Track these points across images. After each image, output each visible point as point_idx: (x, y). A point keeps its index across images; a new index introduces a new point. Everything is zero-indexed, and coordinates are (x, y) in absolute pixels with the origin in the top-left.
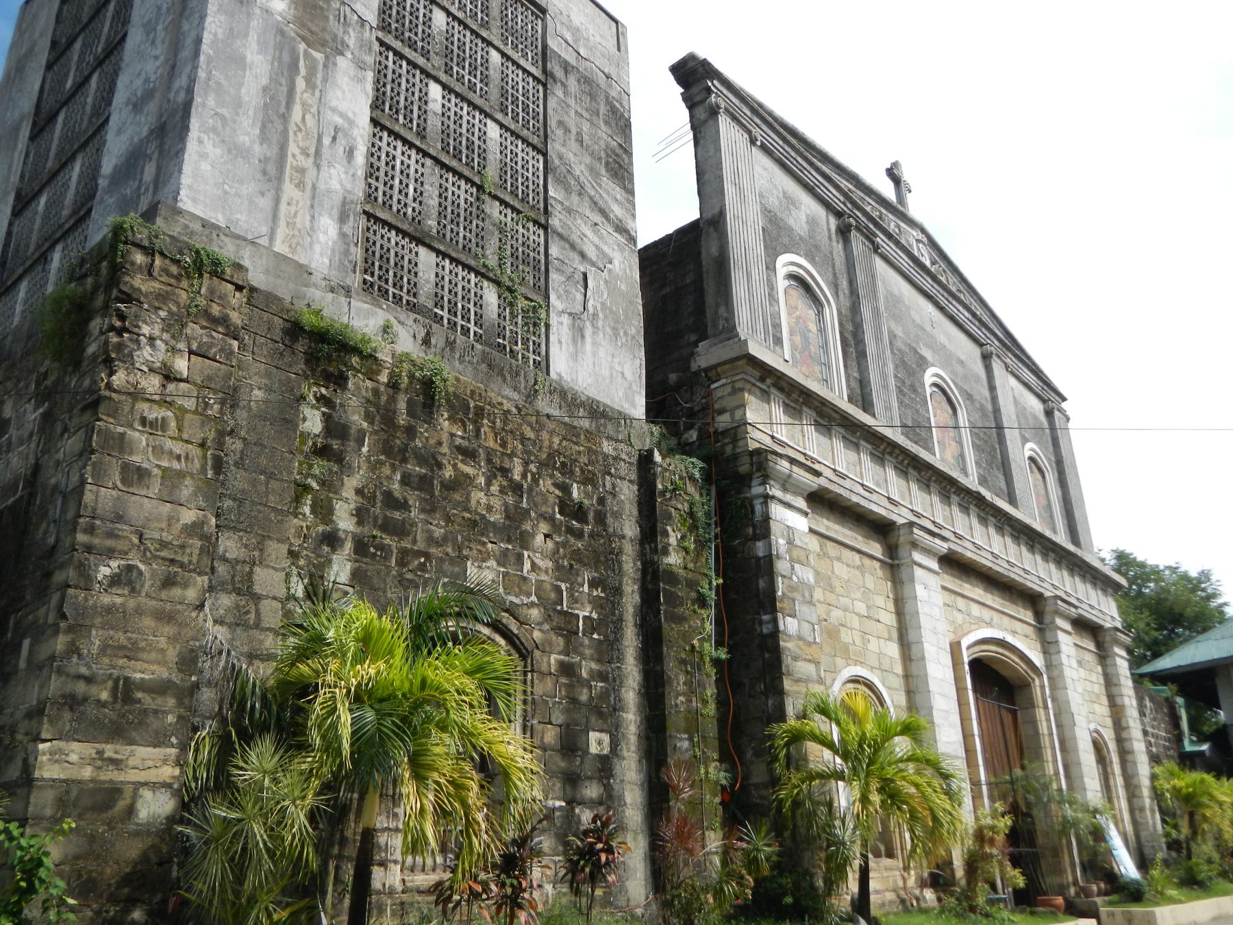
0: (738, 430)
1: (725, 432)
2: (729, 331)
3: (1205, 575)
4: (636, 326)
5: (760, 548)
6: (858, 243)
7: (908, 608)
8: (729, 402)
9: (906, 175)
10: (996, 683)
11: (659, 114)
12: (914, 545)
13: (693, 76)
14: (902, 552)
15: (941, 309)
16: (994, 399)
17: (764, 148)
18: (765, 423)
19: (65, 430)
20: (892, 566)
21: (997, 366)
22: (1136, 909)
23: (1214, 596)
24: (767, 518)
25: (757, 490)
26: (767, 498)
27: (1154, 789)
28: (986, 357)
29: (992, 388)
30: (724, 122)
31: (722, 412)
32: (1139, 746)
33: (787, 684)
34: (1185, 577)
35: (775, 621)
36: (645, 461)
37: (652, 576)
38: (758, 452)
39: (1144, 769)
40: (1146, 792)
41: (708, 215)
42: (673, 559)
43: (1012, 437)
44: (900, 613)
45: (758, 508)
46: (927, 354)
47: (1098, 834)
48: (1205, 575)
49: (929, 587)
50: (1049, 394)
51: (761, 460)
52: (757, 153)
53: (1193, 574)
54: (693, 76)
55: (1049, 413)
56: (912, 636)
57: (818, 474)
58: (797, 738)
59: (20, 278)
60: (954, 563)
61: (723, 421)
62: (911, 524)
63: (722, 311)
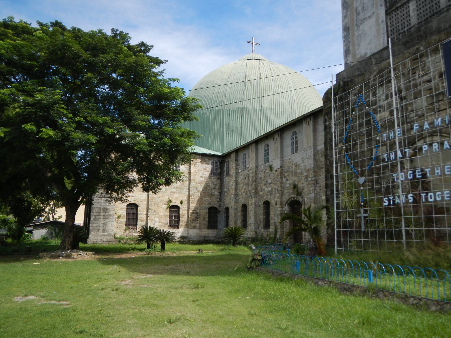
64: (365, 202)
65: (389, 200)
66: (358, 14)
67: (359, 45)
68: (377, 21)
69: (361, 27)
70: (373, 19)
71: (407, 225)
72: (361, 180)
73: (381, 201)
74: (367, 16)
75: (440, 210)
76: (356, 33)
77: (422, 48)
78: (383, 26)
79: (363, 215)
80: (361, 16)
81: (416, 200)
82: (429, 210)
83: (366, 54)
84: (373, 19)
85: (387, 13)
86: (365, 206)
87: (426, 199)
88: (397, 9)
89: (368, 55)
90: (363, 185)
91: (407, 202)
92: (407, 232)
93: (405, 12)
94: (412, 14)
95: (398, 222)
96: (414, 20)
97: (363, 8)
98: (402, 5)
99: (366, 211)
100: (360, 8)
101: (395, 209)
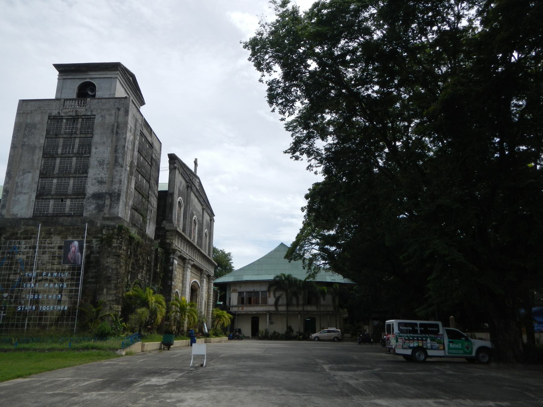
0: (171, 244)
1: (168, 244)
2: (171, 221)
3: (229, 254)
4: (155, 220)
5: (171, 268)
6: (189, 190)
7: (185, 276)
8: (170, 237)
9: (198, 162)
10: (194, 290)
11: (164, 164)
12: (189, 263)
13: (173, 158)
14: (186, 265)
15: (198, 199)
16: (203, 220)
17: (181, 174)
18: (177, 244)
19: (108, 257)
20: (184, 267)
21: (205, 212)
22: (208, 338)
23: (230, 260)
24: (173, 262)
25: (172, 256)
26: (174, 258)
27: (212, 313)
28: (203, 209)
29: (203, 217)
30: (177, 172)
31: (168, 239)
32: (211, 304)
33: (172, 295)
34: (223, 253)
35: (171, 283)
36: (157, 250)
37: (155, 273)
38: (174, 249)
39: (211, 309)
40: (211, 314)
41: (170, 192)
42: (158, 270)
43: (204, 228)
44: (183, 277)
45: (171, 260)
46: (194, 212)
47: (203, 324)
48: (229, 254)
49: (189, 273)
50: (212, 215)
51: (174, 251)
52: (180, 175)
53: (226, 252)
54: (173, 158)
55: (211, 220)
56: (184, 282)
57: (181, 252)
58: (172, 304)
59: (50, 199)
60: (194, 266)
61: (168, 241)
62: (190, 259)
63: (170, 215)
64: (5, 307)
65: (21, 308)
66: (17, 187)
67: (13, 207)
68: (30, 198)
69: (18, 196)
70: (27, 197)
71: (29, 321)
72: (5, 295)
73: (16, 308)
74: (24, 191)
75: (46, 313)
76: (13, 198)
77: (52, 230)
78: (32, 204)
79: (2, 315)
80: (19, 189)
81: (37, 308)
82: (42, 313)
83: (17, 214)
84: (27, 197)
85: (37, 197)
86: (5, 310)
87: (42, 309)
88: (43, 199)
89: (19, 216)
90: (6, 298)
91: (32, 309)
92: (28, 324)
93: (47, 203)
94: (50, 207)
95: (24, 319)
96: (51, 211)
97: (22, 185)
98: (47, 199)
99: (4, 313)
100: (19, 184)
101: (24, 314)
